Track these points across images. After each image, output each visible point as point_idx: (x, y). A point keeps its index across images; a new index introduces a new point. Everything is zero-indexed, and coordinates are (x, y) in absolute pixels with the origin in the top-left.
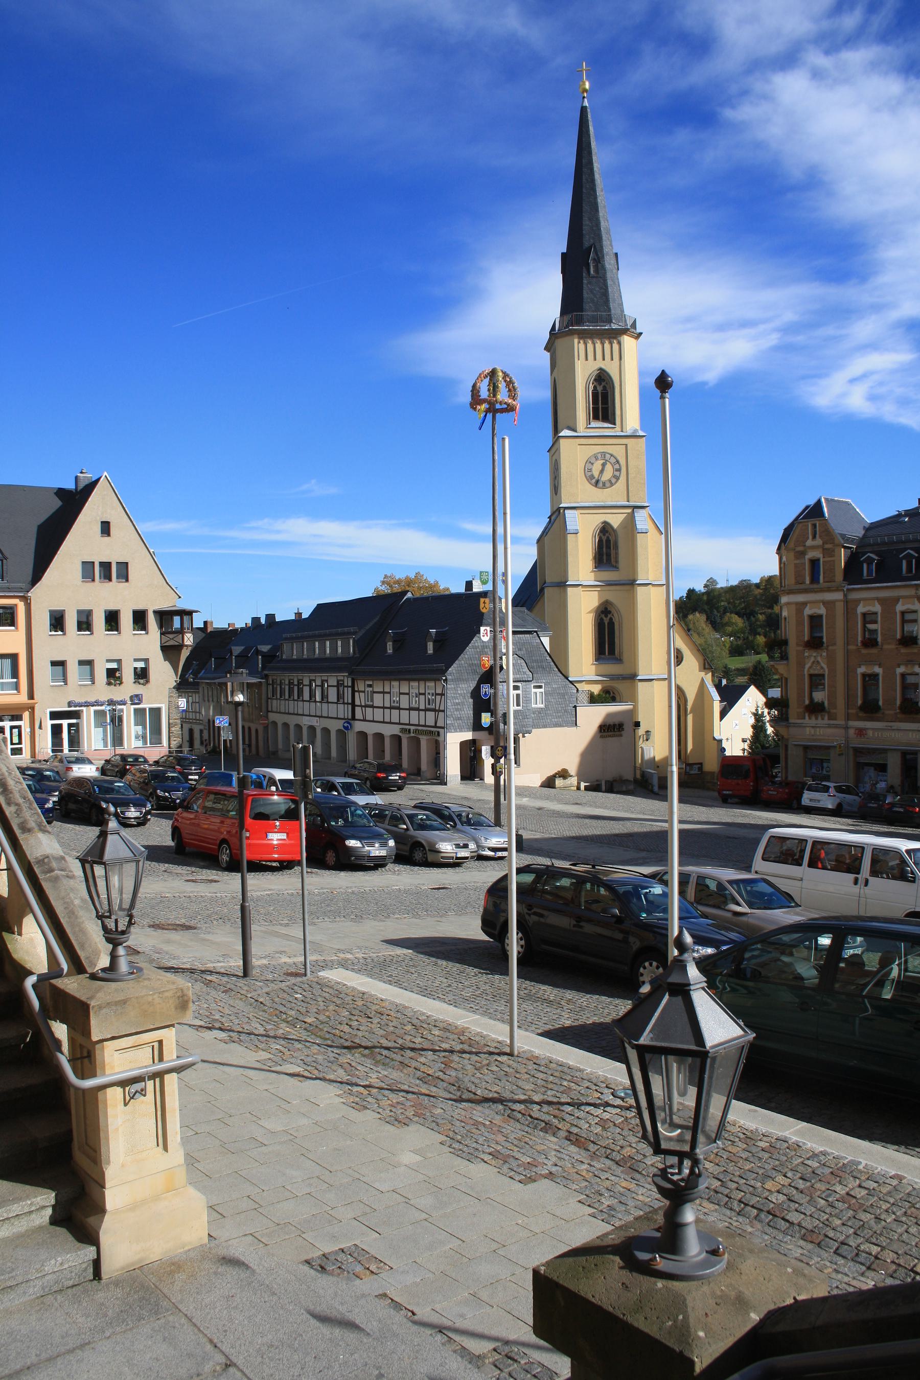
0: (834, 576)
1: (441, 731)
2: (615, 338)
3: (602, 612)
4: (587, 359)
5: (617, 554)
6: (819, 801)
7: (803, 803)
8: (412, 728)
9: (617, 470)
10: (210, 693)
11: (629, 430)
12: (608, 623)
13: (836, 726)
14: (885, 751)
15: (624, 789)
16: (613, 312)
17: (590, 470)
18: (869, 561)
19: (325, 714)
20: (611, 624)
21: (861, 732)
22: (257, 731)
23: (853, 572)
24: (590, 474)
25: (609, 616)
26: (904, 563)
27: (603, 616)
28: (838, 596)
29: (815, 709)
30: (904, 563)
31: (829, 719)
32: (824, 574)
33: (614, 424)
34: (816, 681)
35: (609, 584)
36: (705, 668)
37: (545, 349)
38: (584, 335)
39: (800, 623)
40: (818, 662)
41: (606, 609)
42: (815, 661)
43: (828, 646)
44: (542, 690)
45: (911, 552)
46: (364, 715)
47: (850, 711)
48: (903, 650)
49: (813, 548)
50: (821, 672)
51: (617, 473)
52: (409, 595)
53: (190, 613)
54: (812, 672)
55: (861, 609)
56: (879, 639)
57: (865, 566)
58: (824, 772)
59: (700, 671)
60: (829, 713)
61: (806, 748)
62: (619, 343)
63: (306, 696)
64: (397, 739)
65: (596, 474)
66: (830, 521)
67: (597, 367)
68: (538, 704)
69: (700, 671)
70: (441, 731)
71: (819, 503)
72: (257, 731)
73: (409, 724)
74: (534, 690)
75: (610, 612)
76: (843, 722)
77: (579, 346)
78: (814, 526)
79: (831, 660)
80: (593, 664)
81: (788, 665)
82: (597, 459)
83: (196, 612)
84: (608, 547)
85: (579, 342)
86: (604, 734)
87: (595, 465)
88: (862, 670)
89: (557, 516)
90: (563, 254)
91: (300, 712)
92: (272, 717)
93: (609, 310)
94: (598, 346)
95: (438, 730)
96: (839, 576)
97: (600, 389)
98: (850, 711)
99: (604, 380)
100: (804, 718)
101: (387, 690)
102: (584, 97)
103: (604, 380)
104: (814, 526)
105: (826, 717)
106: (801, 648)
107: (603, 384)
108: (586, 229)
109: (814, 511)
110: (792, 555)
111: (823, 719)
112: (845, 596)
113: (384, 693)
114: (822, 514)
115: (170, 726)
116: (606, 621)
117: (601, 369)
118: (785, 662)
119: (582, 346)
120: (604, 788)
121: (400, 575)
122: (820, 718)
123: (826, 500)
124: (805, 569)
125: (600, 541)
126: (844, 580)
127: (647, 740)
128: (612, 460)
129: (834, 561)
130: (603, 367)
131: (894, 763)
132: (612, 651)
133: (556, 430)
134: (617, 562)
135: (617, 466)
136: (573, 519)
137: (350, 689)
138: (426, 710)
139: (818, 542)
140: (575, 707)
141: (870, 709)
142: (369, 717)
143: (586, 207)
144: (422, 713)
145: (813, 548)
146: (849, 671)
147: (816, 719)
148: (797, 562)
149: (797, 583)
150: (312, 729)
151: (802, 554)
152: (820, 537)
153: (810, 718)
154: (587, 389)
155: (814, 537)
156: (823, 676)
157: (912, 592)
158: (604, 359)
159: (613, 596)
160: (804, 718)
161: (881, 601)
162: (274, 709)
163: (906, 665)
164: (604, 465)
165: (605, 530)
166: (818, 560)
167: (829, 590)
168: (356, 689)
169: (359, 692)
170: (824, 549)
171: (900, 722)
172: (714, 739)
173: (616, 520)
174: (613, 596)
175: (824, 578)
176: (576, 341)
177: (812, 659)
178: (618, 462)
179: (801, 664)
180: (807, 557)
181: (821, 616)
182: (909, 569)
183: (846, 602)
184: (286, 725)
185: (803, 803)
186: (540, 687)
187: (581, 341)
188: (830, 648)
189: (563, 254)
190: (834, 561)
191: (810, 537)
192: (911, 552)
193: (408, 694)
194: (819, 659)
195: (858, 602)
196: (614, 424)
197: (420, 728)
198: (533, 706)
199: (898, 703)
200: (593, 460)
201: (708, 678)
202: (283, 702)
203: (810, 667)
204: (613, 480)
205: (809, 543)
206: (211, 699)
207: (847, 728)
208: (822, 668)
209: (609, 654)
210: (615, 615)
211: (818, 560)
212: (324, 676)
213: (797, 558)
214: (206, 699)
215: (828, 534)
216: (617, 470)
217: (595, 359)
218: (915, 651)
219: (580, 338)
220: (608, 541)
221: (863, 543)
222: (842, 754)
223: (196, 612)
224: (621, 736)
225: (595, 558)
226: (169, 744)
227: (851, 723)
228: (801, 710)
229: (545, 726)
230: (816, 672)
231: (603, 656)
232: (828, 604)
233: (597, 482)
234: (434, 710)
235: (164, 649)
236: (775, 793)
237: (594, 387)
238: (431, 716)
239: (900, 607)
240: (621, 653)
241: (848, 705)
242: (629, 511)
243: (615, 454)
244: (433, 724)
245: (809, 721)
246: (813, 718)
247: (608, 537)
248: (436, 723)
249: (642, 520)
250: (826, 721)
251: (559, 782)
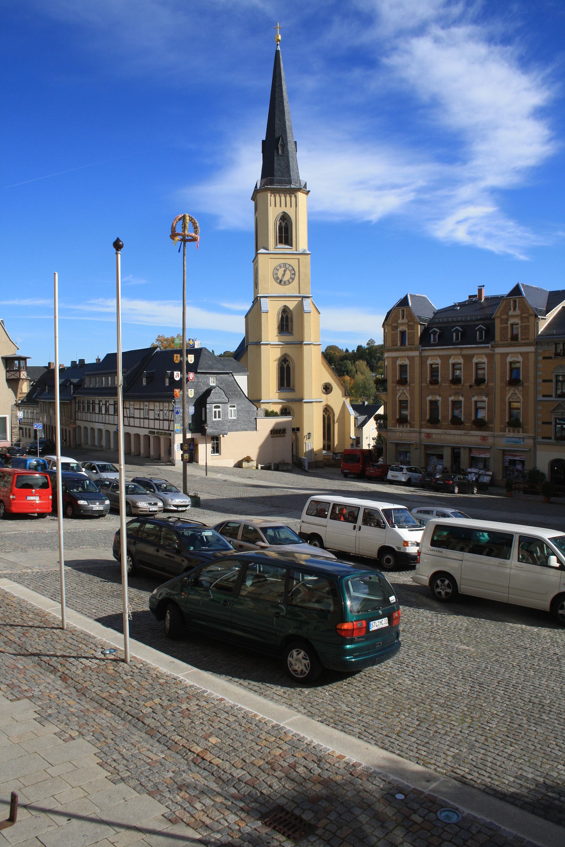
0: (414, 341)
1: (172, 433)
2: (293, 193)
3: (283, 361)
4: (275, 206)
5: (292, 325)
6: (397, 477)
7: (388, 478)
8: (156, 431)
9: (293, 274)
10: (45, 408)
11: (300, 250)
12: (286, 367)
13: (414, 432)
14: (442, 447)
15: (286, 468)
16: (292, 177)
17: (277, 274)
18: (435, 333)
19: (107, 422)
20: (288, 368)
21: (428, 435)
22: (69, 431)
23: (425, 339)
24: (276, 276)
25: (287, 363)
26: (454, 334)
27: (283, 363)
28: (416, 353)
29: (403, 420)
30: (454, 334)
31: (410, 427)
32: (408, 340)
33: (292, 246)
34: (403, 404)
35: (287, 343)
36: (345, 395)
37: (252, 199)
38: (274, 192)
39: (394, 369)
40: (404, 393)
41: (285, 359)
42: (403, 393)
43: (410, 384)
44: (235, 408)
45: (459, 328)
46: (129, 422)
47: (422, 423)
48: (453, 387)
49: (402, 324)
50: (406, 399)
51: (293, 276)
52: (158, 349)
53: (25, 359)
54: (401, 399)
55: (429, 362)
56: (439, 380)
57: (432, 336)
58: (408, 459)
59: (343, 397)
60: (410, 423)
61: (397, 445)
62: (296, 197)
63: (97, 410)
64: (147, 437)
65: (280, 277)
66: (412, 309)
67: (282, 211)
68: (232, 416)
69: (343, 397)
70: (172, 433)
71: (406, 297)
72: (69, 431)
73: (154, 429)
74: (230, 409)
75: (287, 361)
76: (418, 429)
77: (271, 198)
78: (403, 311)
79: (412, 393)
80: (277, 392)
81: (387, 394)
82: (281, 267)
83: (29, 358)
84: (287, 320)
85: (271, 196)
86: (274, 435)
87: (279, 271)
88: (429, 398)
89: (257, 301)
90: (263, 141)
91: (94, 420)
92: (79, 423)
93: (290, 176)
94: (283, 198)
95: (170, 432)
96: (417, 342)
97: (283, 224)
98: (422, 423)
99: (286, 219)
100: (396, 427)
101: (142, 407)
102: (278, 45)
103: (286, 219)
104: (403, 311)
105: (409, 426)
106: (395, 385)
107: (286, 221)
108: (277, 126)
109: (404, 302)
110: (390, 328)
111: (407, 427)
112: (420, 353)
113: (140, 409)
114: (408, 304)
115: (12, 428)
116: (285, 366)
117: (284, 212)
118: (385, 393)
119: (273, 198)
120: (273, 468)
121: (168, 336)
122: (405, 426)
123: (411, 295)
124: (397, 337)
125: (282, 317)
126: (419, 344)
127: (309, 438)
128: (290, 268)
129: (414, 332)
130: (286, 211)
131: (447, 454)
132: (288, 384)
133: (257, 249)
134: (292, 330)
135: (293, 272)
136: (265, 304)
138: (164, 420)
139: (405, 320)
140: (256, 419)
141: (434, 421)
142: (132, 424)
143: (277, 113)
144: (161, 422)
145: (402, 324)
146: (422, 399)
147: (403, 427)
148: (393, 332)
149: (393, 345)
150: (100, 430)
151: (396, 328)
152: (407, 318)
153: (399, 427)
154: (275, 224)
155: (403, 318)
156: (407, 401)
157: (458, 352)
158: (286, 206)
159: (290, 351)
160: (396, 427)
161: (441, 357)
162: (79, 419)
163: (455, 396)
164: (285, 271)
165: (285, 310)
166: (405, 332)
167: (411, 350)
170: (408, 325)
171: (451, 429)
172: (351, 438)
173: (292, 305)
174: (290, 351)
175: (408, 342)
176: (269, 195)
177: (401, 391)
178: (293, 269)
179: (394, 394)
180: (399, 330)
181: (406, 365)
182: (457, 338)
183: (421, 357)
184: (86, 428)
185: (388, 478)
186: (234, 406)
187: (273, 195)
188: (411, 384)
189: (263, 141)
190: (414, 332)
191: (401, 318)
192: (459, 328)
194: (405, 391)
195: (428, 357)
196: (292, 246)
197: (160, 431)
198: (229, 418)
199: (450, 418)
200: (278, 268)
201: (348, 401)
202: (84, 414)
203: (400, 396)
204: (291, 281)
205: (400, 321)
206: (45, 411)
207: (420, 433)
208: (406, 396)
209: (287, 386)
210: (291, 362)
211: (405, 332)
212: (107, 398)
213: (393, 330)
214: (43, 411)
215: (411, 316)
216: (293, 274)
217: (281, 206)
218: (460, 387)
219: (271, 193)
220: (287, 317)
221: (432, 323)
222: (418, 448)
223: (29, 358)
224: (284, 436)
225: (279, 328)
226: (12, 440)
227: (423, 430)
228: (394, 422)
229: (237, 431)
230: (403, 399)
231: (283, 387)
232: (411, 359)
233: (281, 281)
234: (168, 420)
235: (8, 381)
236: (373, 472)
237: (280, 223)
238: (166, 423)
239: (452, 361)
240: (294, 386)
241: (421, 420)
242: (300, 299)
243: (292, 264)
244: (167, 429)
245: (398, 428)
246: (401, 426)
247: (287, 315)
248: (169, 428)
249: (308, 305)
250: (408, 429)
251: (245, 464)
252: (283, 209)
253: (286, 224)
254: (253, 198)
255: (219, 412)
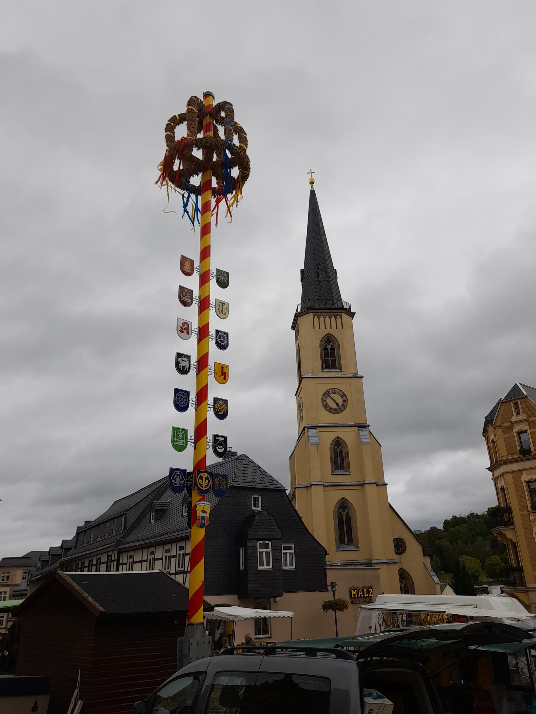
3: (340, 508)
5: (348, 461)
25: (346, 510)
33: (342, 370)
44: (292, 551)
68: (289, 565)
74: (283, 551)
113: (142, 561)
116: (344, 514)
125: (335, 452)
130: (330, 333)
134: (349, 468)
137: (115, 562)
165: (338, 443)
168: (121, 562)
169: (123, 564)
187: (316, 317)
193: (161, 559)
220: (341, 452)
240: (358, 541)
247: (341, 449)
252: (328, 331)
253: (332, 346)
254: (294, 326)
255: (267, 553)
